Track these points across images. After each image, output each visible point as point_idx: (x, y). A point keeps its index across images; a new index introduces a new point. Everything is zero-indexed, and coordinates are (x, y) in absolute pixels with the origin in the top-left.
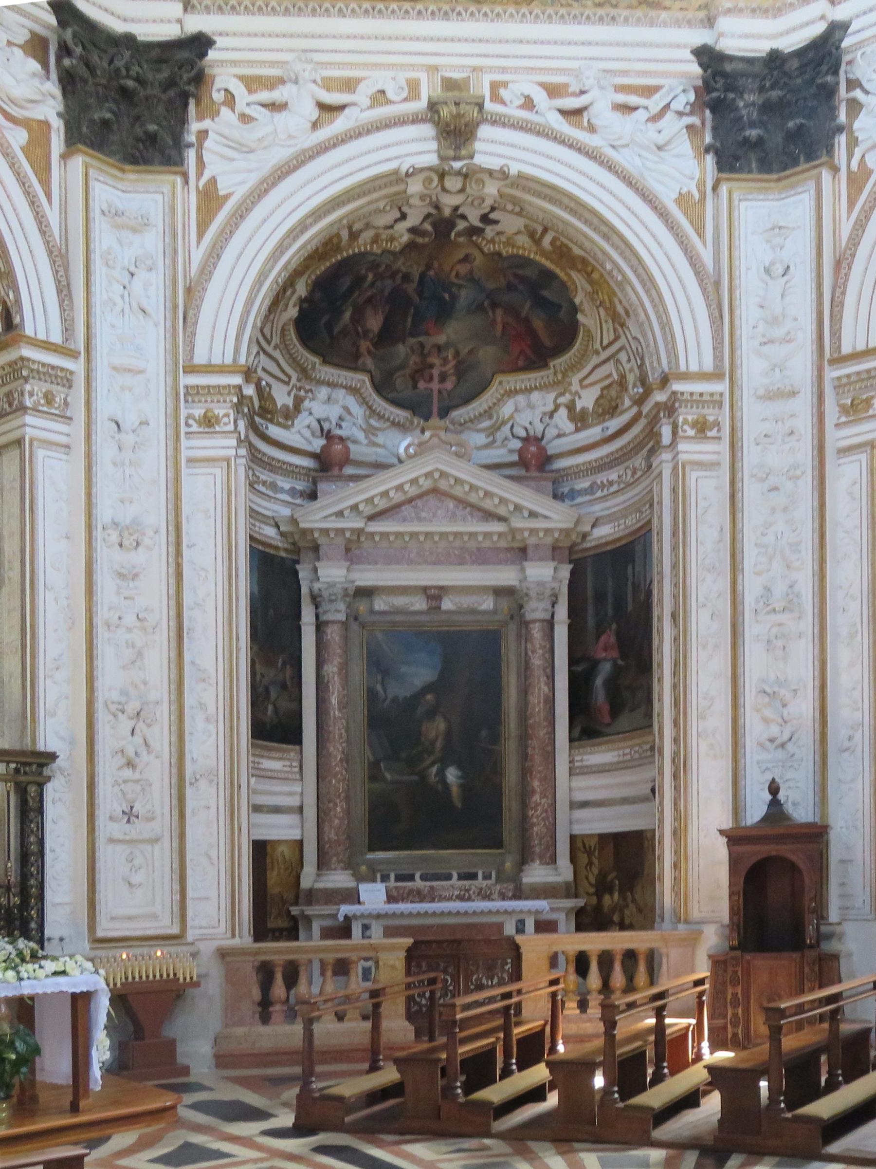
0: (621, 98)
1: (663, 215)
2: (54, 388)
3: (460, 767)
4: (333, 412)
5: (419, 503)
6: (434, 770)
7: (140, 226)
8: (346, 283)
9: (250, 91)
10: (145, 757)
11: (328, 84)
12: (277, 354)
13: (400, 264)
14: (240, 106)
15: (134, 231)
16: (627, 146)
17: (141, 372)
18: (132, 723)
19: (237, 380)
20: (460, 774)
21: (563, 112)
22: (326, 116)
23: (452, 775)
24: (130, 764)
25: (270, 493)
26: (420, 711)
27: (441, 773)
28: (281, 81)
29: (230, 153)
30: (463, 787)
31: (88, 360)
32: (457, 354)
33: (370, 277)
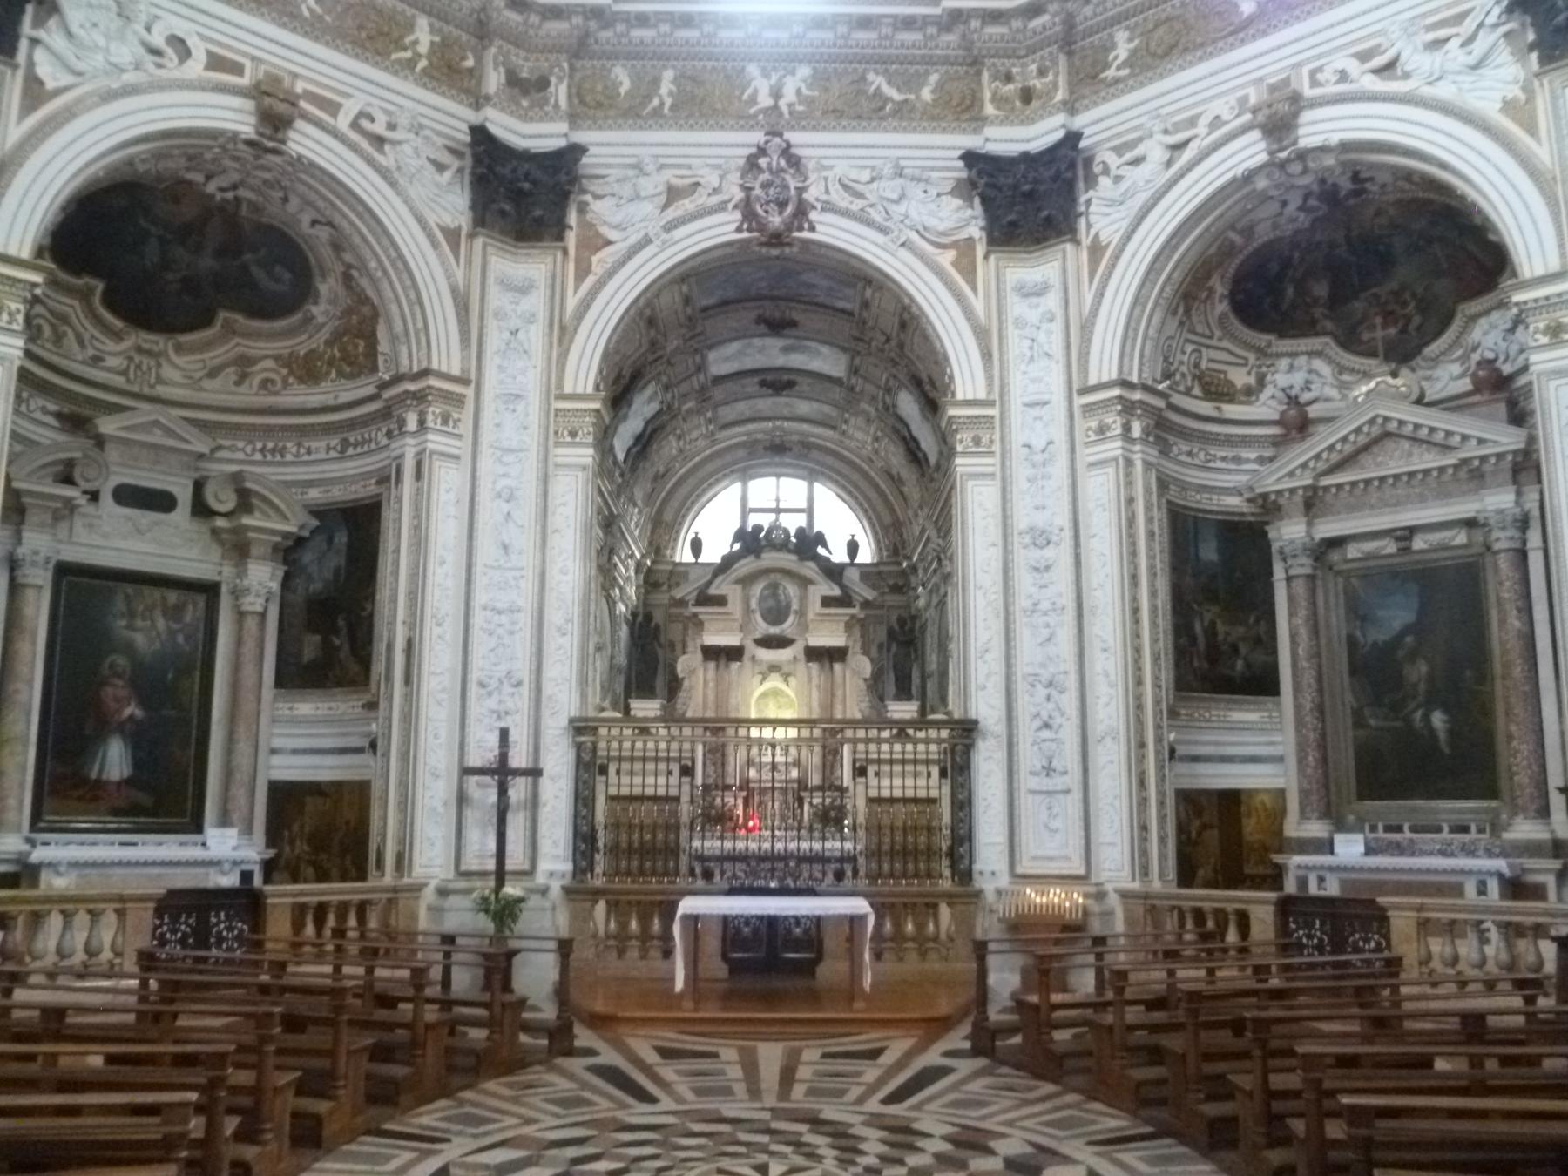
0: (1431, 36)
1: (1486, 128)
2: (980, 433)
3: (1446, 709)
4: (1298, 379)
5: (1375, 449)
6: (1419, 714)
7: (1040, 291)
8: (1274, 267)
9: (1120, 155)
10: (1058, 720)
11: (1178, 127)
12: (1225, 344)
13: (1318, 237)
14: (1113, 172)
15: (1039, 294)
16: (1439, 79)
17: (1046, 403)
18: (1046, 691)
19: (1116, 392)
20: (1445, 717)
21: (1377, 71)
22: (1176, 153)
23: (1438, 719)
24: (1047, 726)
25: (1233, 467)
26: (1401, 653)
27: (1426, 718)
28: (1140, 140)
29: (1107, 210)
30: (1451, 732)
31: (1002, 405)
32: (1414, 295)
33: (1297, 255)
